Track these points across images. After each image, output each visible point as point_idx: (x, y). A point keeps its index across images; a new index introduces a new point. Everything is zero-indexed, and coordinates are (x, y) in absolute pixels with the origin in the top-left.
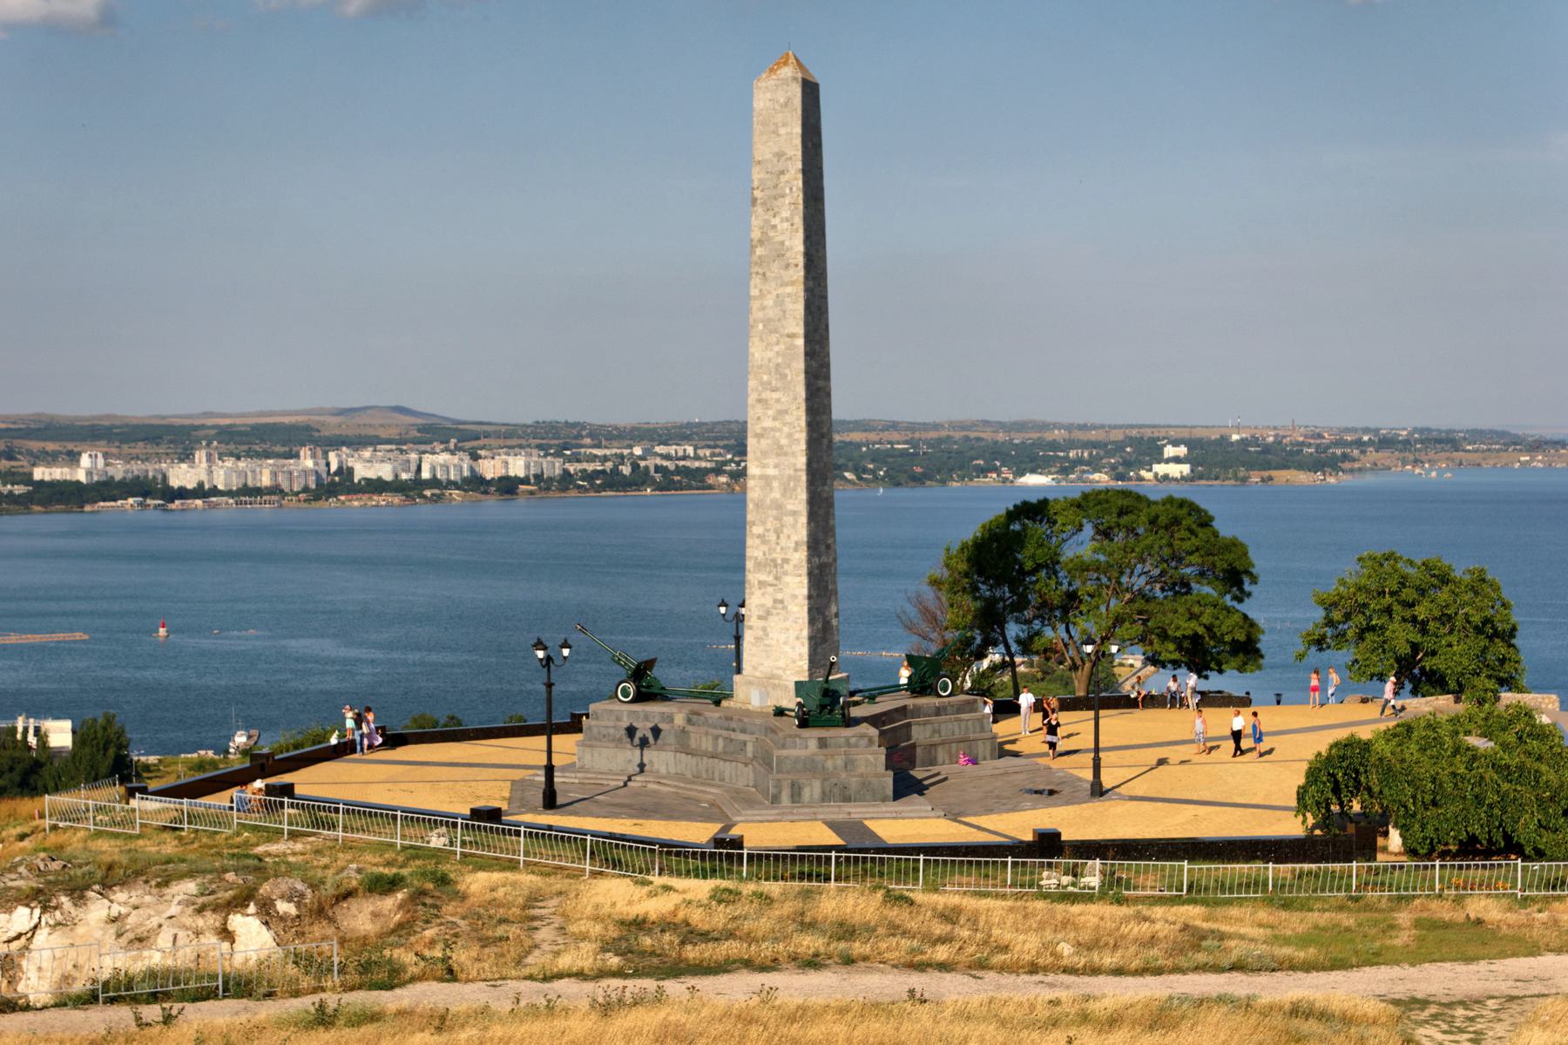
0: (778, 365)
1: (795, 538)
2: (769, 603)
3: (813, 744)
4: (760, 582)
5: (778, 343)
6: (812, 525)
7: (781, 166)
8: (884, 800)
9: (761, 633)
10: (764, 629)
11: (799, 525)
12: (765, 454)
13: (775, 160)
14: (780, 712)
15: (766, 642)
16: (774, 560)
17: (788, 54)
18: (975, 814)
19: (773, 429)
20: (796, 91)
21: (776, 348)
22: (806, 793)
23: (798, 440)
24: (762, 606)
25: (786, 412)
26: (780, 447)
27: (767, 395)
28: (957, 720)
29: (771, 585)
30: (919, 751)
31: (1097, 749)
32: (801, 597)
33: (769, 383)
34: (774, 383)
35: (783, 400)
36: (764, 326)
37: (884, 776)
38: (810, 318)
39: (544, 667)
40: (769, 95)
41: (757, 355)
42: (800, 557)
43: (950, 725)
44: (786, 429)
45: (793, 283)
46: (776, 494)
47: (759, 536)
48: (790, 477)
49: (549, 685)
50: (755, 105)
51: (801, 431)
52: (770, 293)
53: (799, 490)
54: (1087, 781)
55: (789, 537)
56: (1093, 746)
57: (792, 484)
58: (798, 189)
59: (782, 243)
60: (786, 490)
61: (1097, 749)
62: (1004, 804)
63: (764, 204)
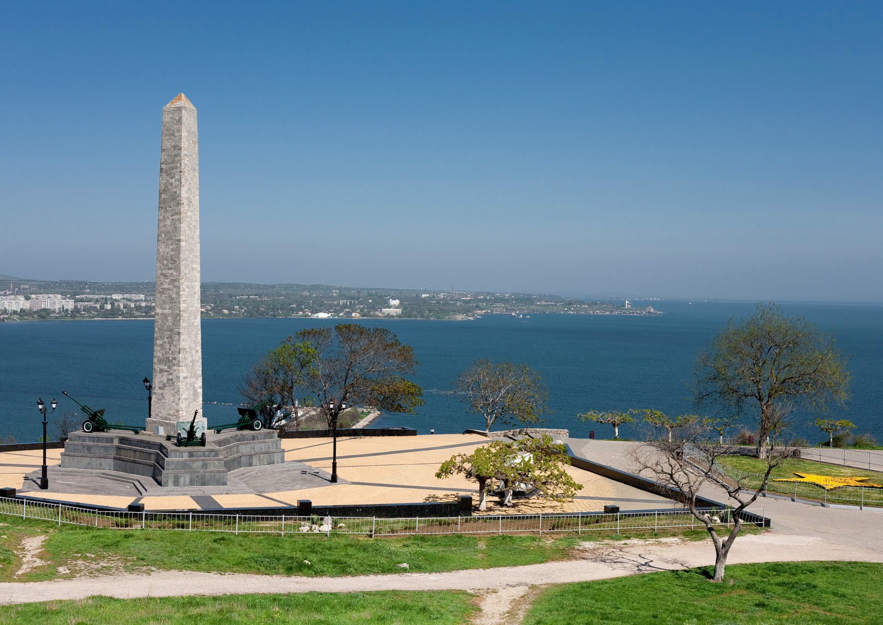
2: (165, 380)
3: (186, 455)
7: (176, 152)
10: (162, 394)
12: (164, 302)
13: (173, 149)
15: (163, 401)
16: (168, 358)
19: (169, 289)
21: (171, 247)
22: (182, 480)
28: (263, 442)
29: (166, 371)
30: (243, 459)
31: (335, 458)
33: (168, 266)
34: (169, 265)
39: (42, 413)
40: (170, 116)
43: (260, 445)
44: (175, 290)
47: (160, 345)
49: (45, 424)
52: (168, 218)
54: (329, 474)
56: (333, 456)
57: (178, 318)
59: (175, 192)
61: (335, 458)
63: (166, 171)
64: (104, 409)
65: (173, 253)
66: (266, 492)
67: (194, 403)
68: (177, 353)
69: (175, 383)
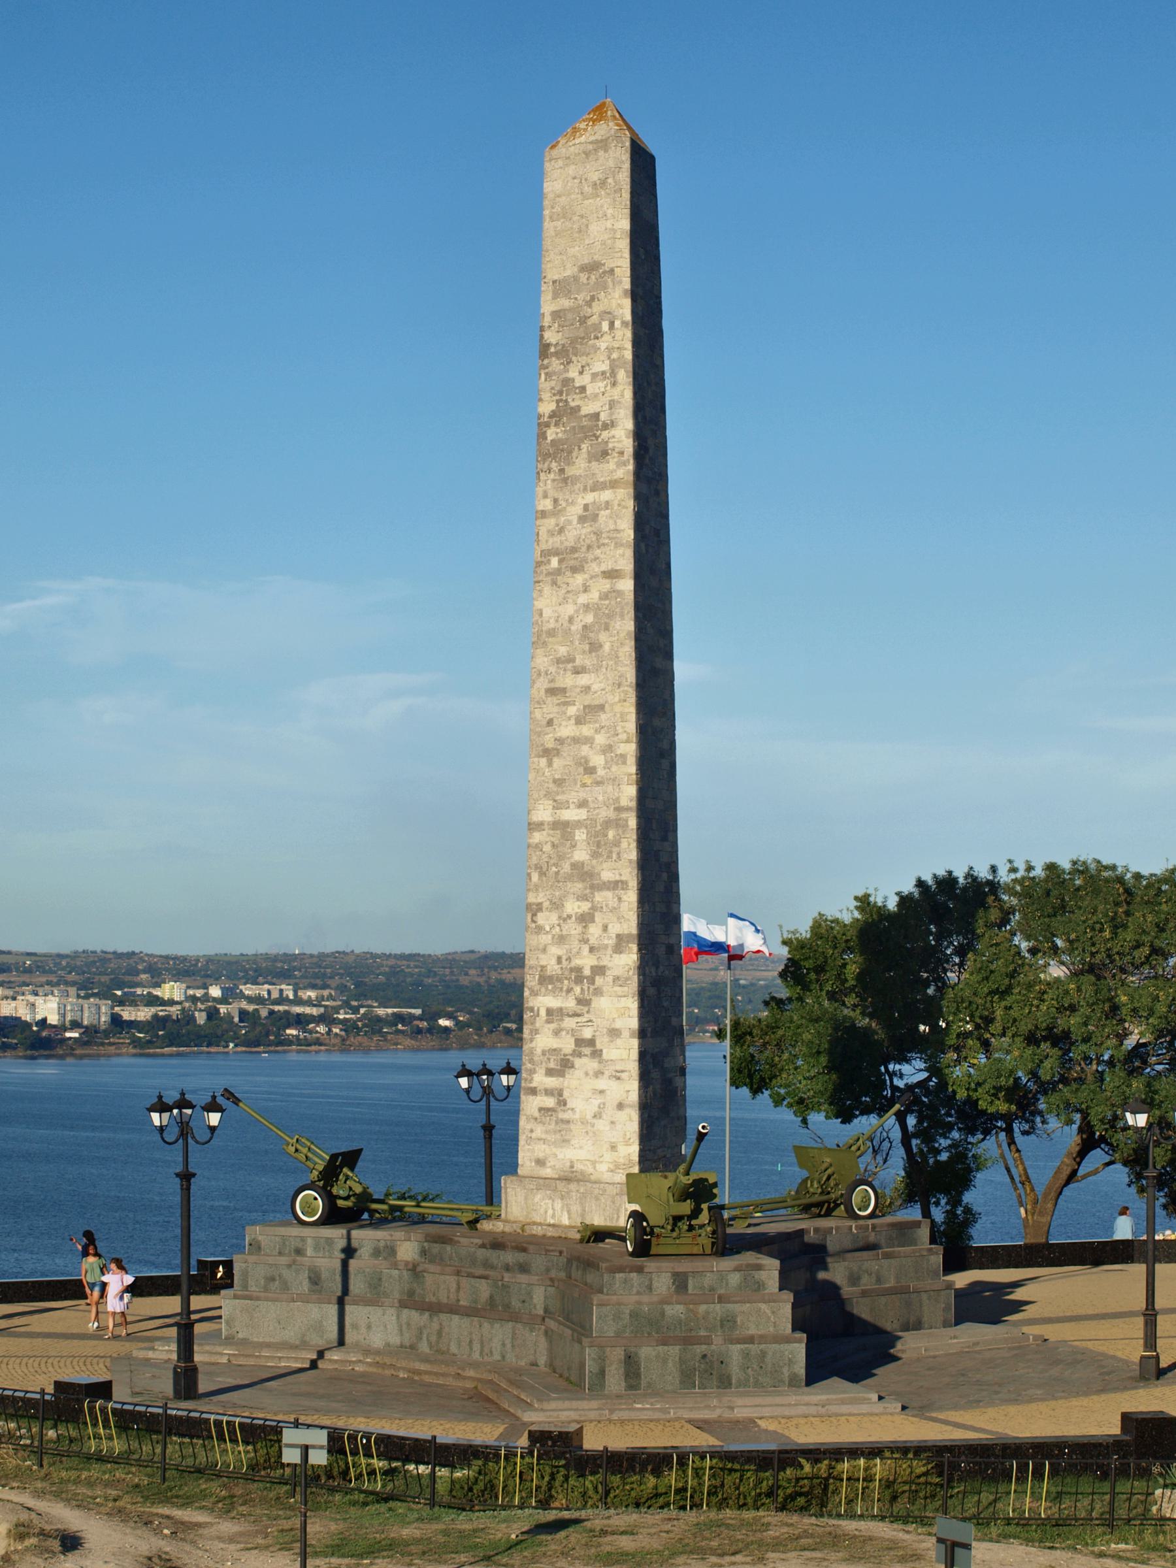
0: (585, 627)
1: (615, 929)
2: (567, 1045)
4: (549, 1012)
5: (586, 589)
6: (647, 907)
8: (951, 1326)
9: (550, 1102)
10: (558, 1093)
11: (624, 906)
14: (599, 1235)
15: (562, 1115)
16: (579, 970)
17: (603, 104)
18: (956, 1407)
19: (576, 740)
20: (620, 158)
21: (583, 599)
23: (623, 757)
24: (555, 1051)
25: (601, 708)
26: (591, 771)
27: (568, 680)
32: (626, 1034)
33: (573, 660)
34: (578, 662)
35: (595, 687)
36: (560, 561)
37: (787, 1340)
38: (643, 545)
41: (547, 613)
42: (630, 958)
45: (614, 484)
46: (581, 855)
48: (608, 823)
49: (186, 1177)
50: (548, 187)
51: (628, 741)
53: (624, 844)
55: (605, 928)
57: (611, 834)
58: (624, 323)
60: (600, 847)
62: (997, 1393)
64: (362, 1150)
65: (589, 619)
66: (941, 1409)
67: (663, 1123)
68: (609, 951)
69: (604, 1051)
